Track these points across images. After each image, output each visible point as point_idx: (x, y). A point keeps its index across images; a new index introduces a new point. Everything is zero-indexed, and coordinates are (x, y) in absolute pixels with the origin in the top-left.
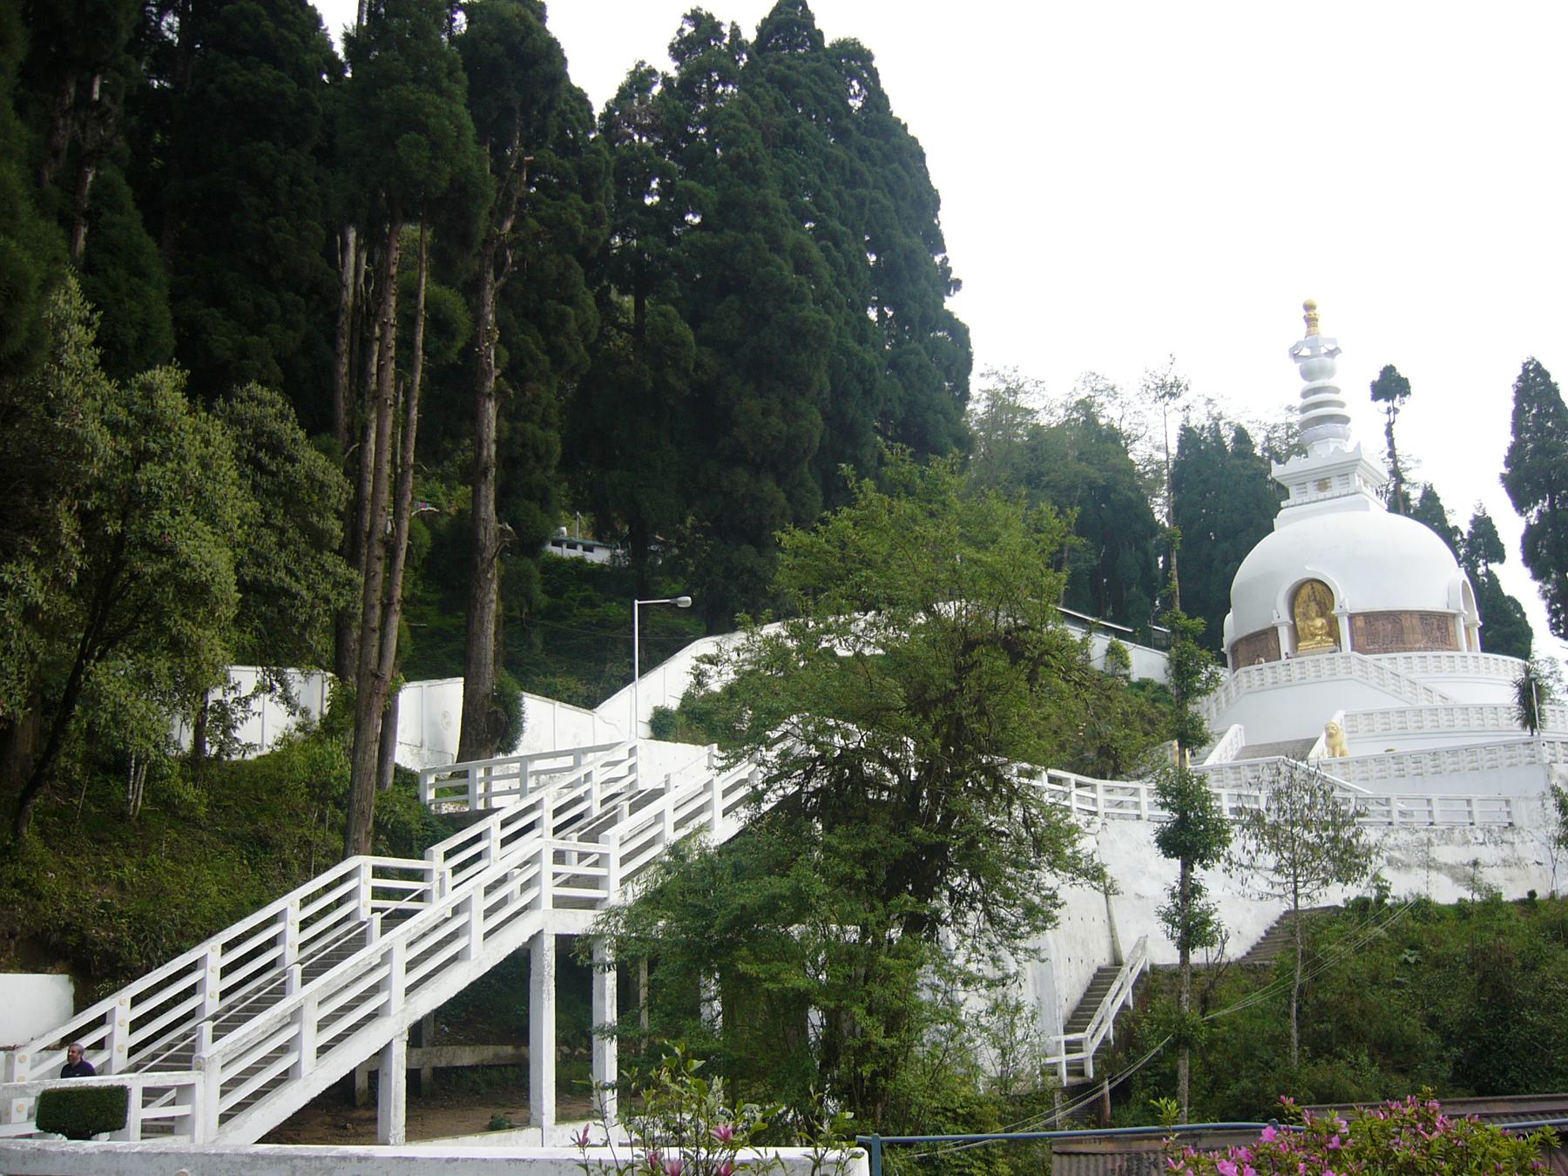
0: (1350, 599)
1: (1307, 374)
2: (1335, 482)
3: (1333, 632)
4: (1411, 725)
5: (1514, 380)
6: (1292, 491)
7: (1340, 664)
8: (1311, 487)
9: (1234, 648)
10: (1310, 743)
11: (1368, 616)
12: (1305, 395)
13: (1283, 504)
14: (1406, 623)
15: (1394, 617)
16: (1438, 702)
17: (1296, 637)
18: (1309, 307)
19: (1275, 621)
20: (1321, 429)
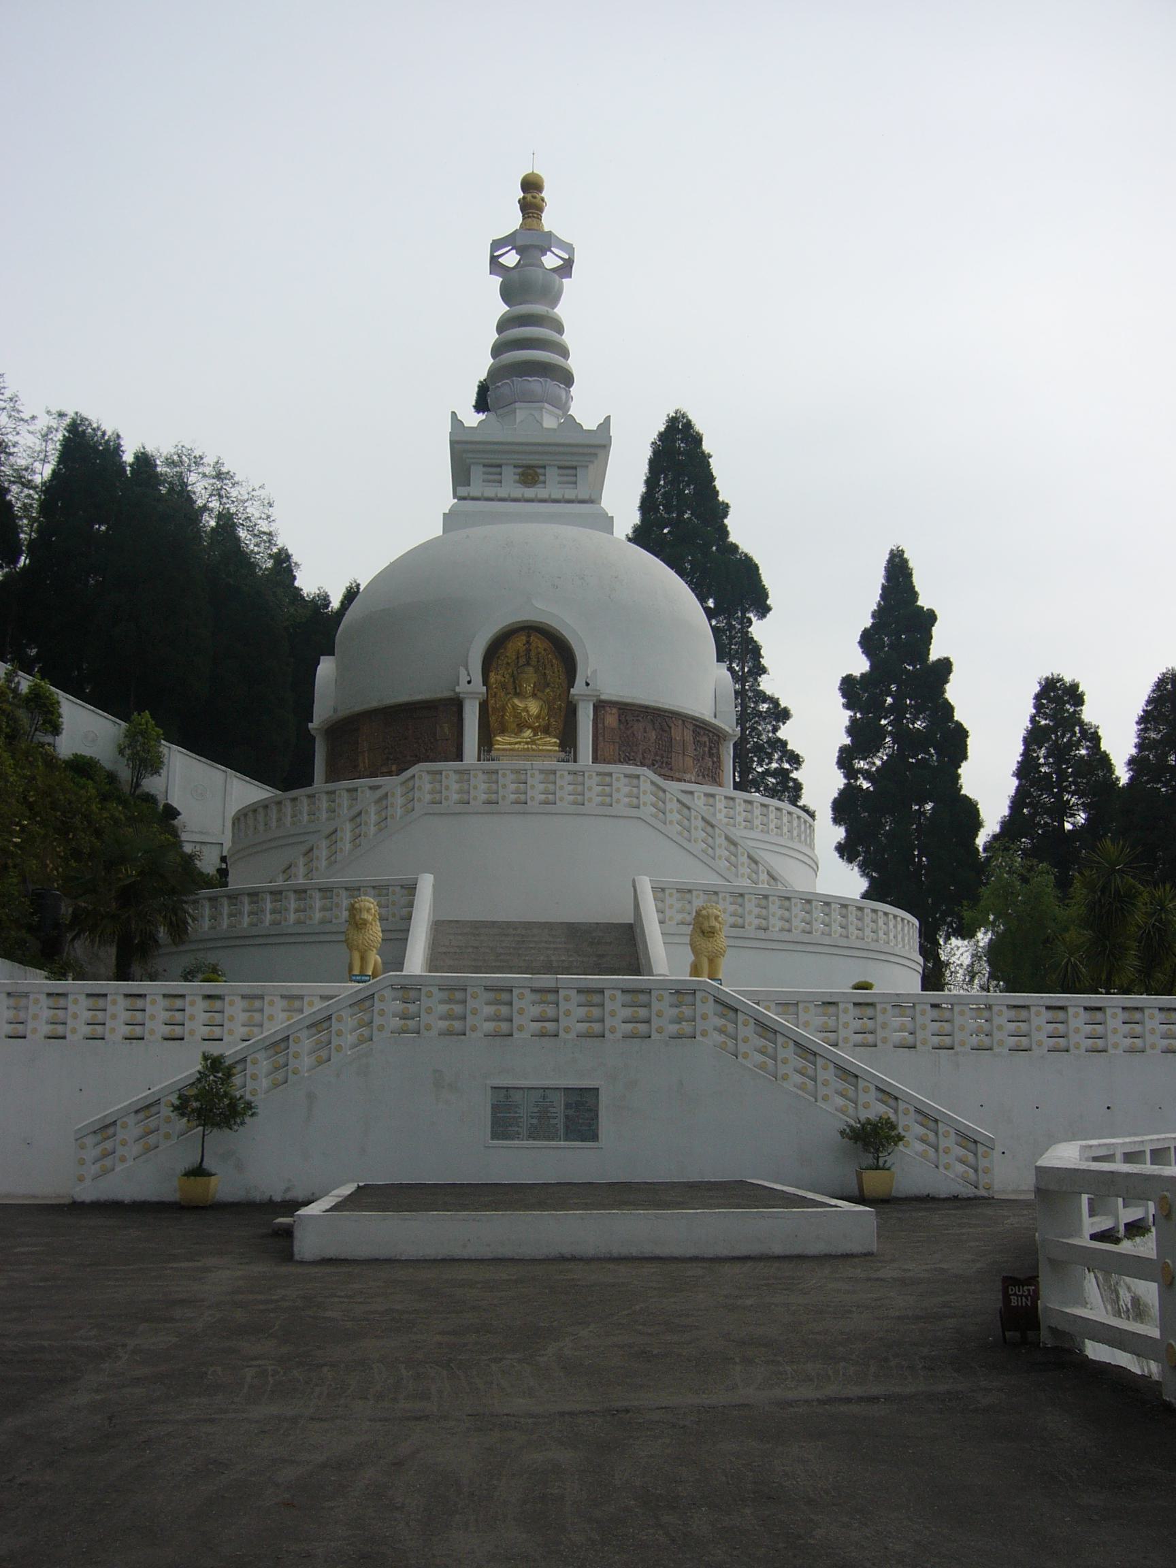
0: (605, 673)
1: (507, 294)
2: (552, 474)
4: (752, 921)
5: (653, 436)
7: (564, 782)
8: (509, 474)
9: (345, 730)
11: (630, 712)
12: (502, 326)
14: (676, 733)
15: (661, 719)
16: (764, 885)
18: (531, 185)
19: (462, 688)
20: (535, 384)
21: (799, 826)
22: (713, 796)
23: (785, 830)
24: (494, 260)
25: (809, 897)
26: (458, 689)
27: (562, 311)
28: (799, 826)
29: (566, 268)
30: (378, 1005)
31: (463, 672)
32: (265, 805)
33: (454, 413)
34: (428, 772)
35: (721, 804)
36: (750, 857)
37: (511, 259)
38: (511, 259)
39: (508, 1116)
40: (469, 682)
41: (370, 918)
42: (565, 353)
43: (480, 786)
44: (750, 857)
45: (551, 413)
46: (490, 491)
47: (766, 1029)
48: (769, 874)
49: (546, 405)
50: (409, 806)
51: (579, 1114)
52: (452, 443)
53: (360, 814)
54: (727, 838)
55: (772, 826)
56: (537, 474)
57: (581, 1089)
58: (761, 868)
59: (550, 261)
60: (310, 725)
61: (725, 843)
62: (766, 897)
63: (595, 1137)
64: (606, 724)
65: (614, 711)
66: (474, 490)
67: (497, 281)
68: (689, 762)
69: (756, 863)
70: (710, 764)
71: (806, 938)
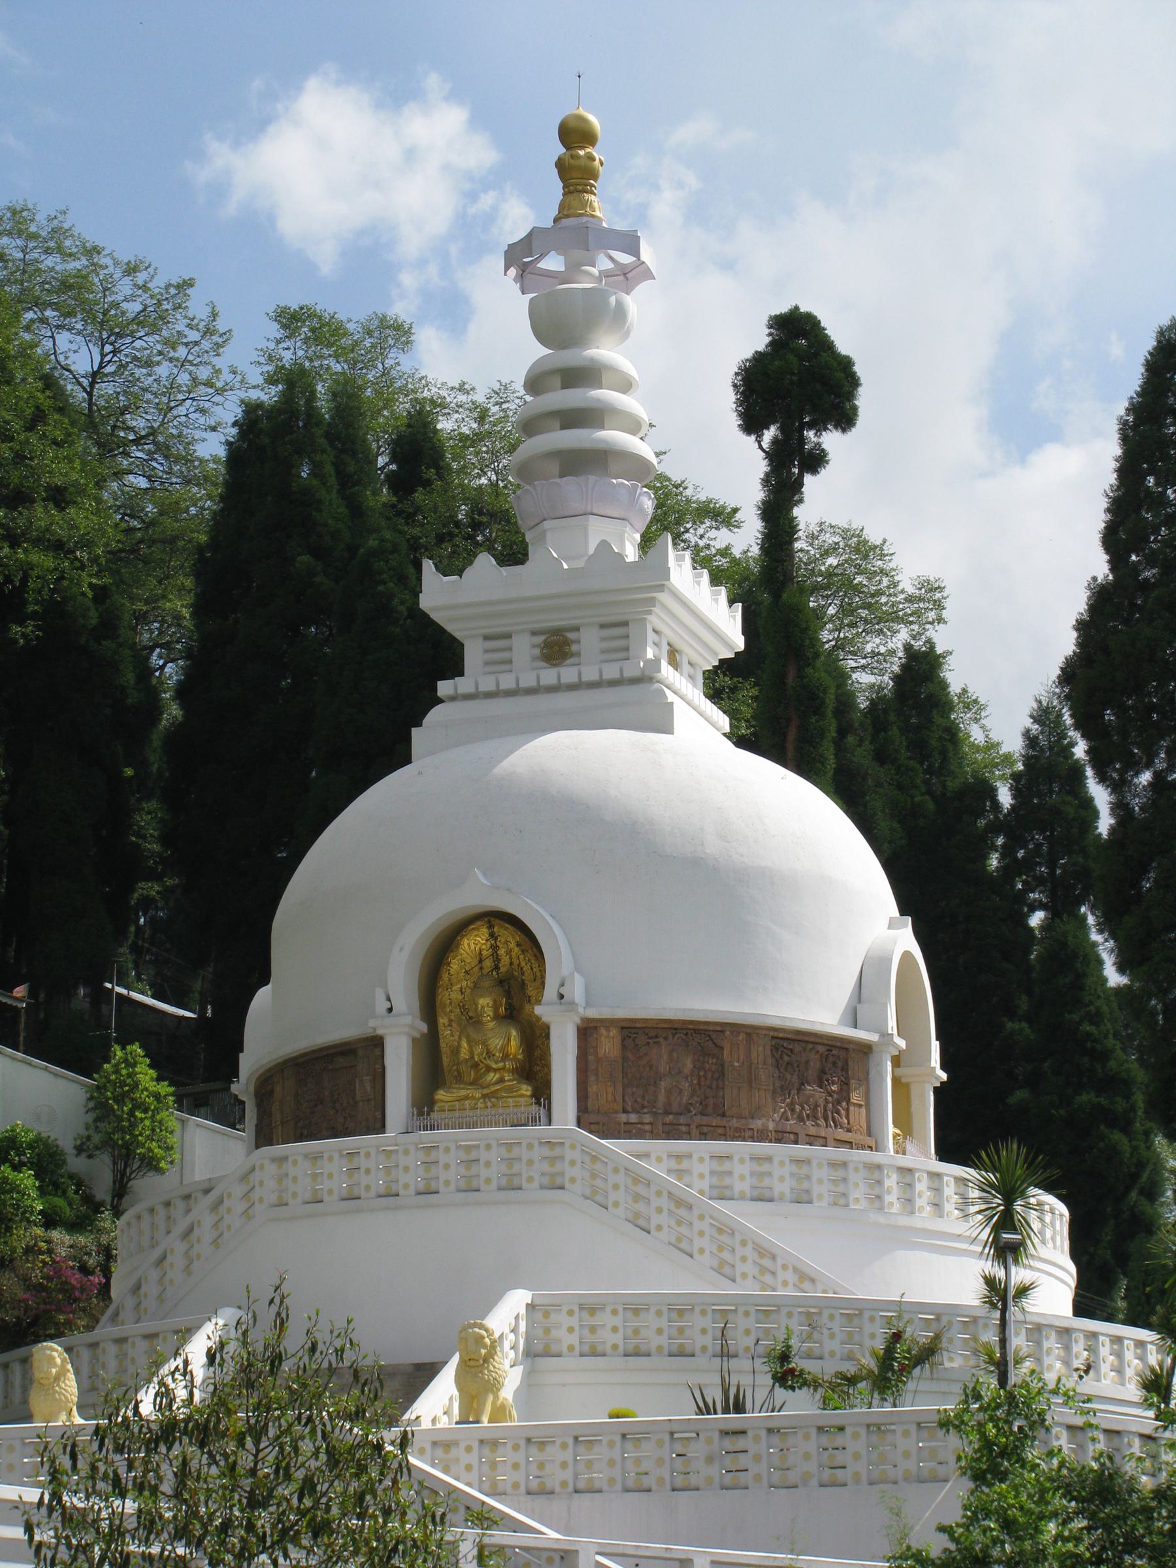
2: (589, 641)
3: (534, 1071)
6: (473, 656)
8: (524, 648)
10: (424, 1374)
13: (444, 688)
17: (433, 1072)
18: (575, 135)
40: (390, 1010)
56: (568, 643)
64: (601, 1053)
65: (614, 1032)
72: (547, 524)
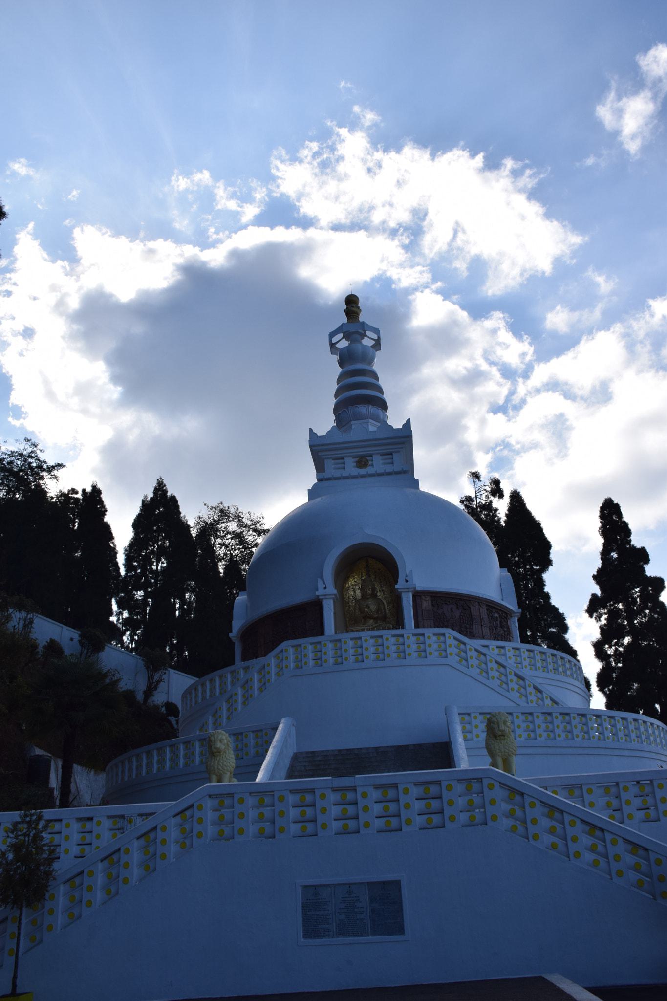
1: (341, 363)
8: (350, 463)
14: (475, 611)
19: (320, 592)
20: (363, 409)
21: (571, 668)
22: (503, 647)
23: (561, 670)
24: (332, 346)
25: (584, 712)
26: (317, 593)
27: (376, 367)
28: (571, 668)
29: (377, 345)
30: (197, 814)
31: (320, 581)
32: (194, 687)
33: (311, 430)
34: (292, 646)
35: (510, 653)
36: (535, 688)
37: (344, 344)
38: (344, 344)
39: (324, 912)
40: (325, 588)
41: (223, 747)
42: (381, 390)
43: (330, 649)
44: (535, 688)
45: (374, 425)
46: (338, 474)
47: (553, 810)
48: (551, 699)
49: (371, 421)
50: (281, 673)
51: (382, 908)
52: (311, 447)
53: (247, 682)
54: (516, 675)
55: (550, 667)
57: (384, 883)
58: (545, 695)
59: (367, 342)
60: (230, 635)
61: (515, 679)
62: (550, 714)
63: (401, 930)
65: (428, 598)
66: (328, 474)
67: (336, 358)
68: (486, 631)
69: (540, 691)
70: (502, 632)
71: (586, 743)
72: (352, 422)
